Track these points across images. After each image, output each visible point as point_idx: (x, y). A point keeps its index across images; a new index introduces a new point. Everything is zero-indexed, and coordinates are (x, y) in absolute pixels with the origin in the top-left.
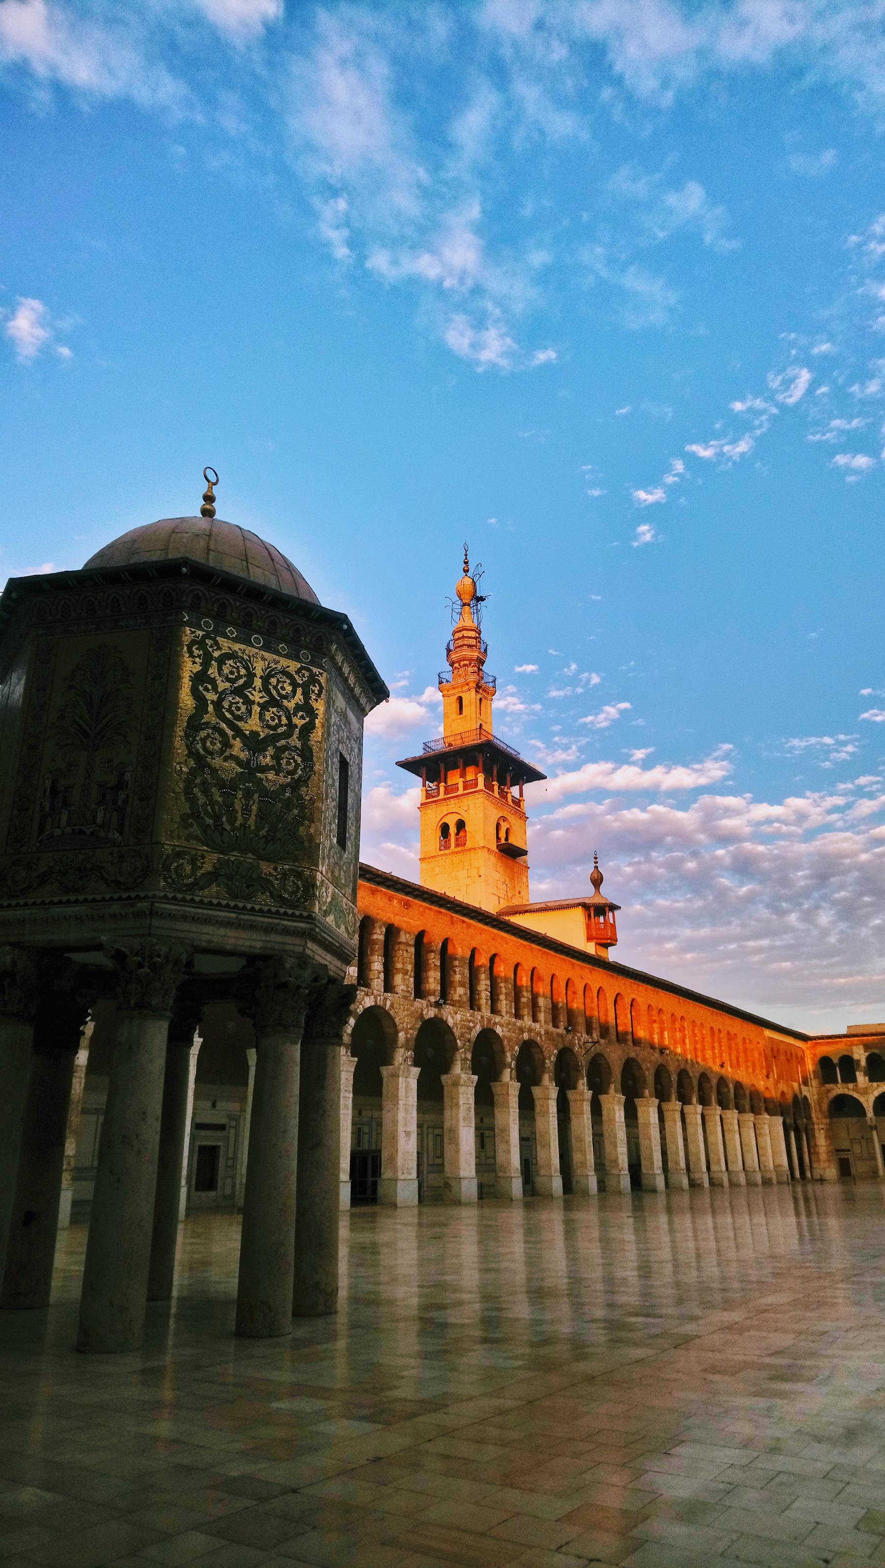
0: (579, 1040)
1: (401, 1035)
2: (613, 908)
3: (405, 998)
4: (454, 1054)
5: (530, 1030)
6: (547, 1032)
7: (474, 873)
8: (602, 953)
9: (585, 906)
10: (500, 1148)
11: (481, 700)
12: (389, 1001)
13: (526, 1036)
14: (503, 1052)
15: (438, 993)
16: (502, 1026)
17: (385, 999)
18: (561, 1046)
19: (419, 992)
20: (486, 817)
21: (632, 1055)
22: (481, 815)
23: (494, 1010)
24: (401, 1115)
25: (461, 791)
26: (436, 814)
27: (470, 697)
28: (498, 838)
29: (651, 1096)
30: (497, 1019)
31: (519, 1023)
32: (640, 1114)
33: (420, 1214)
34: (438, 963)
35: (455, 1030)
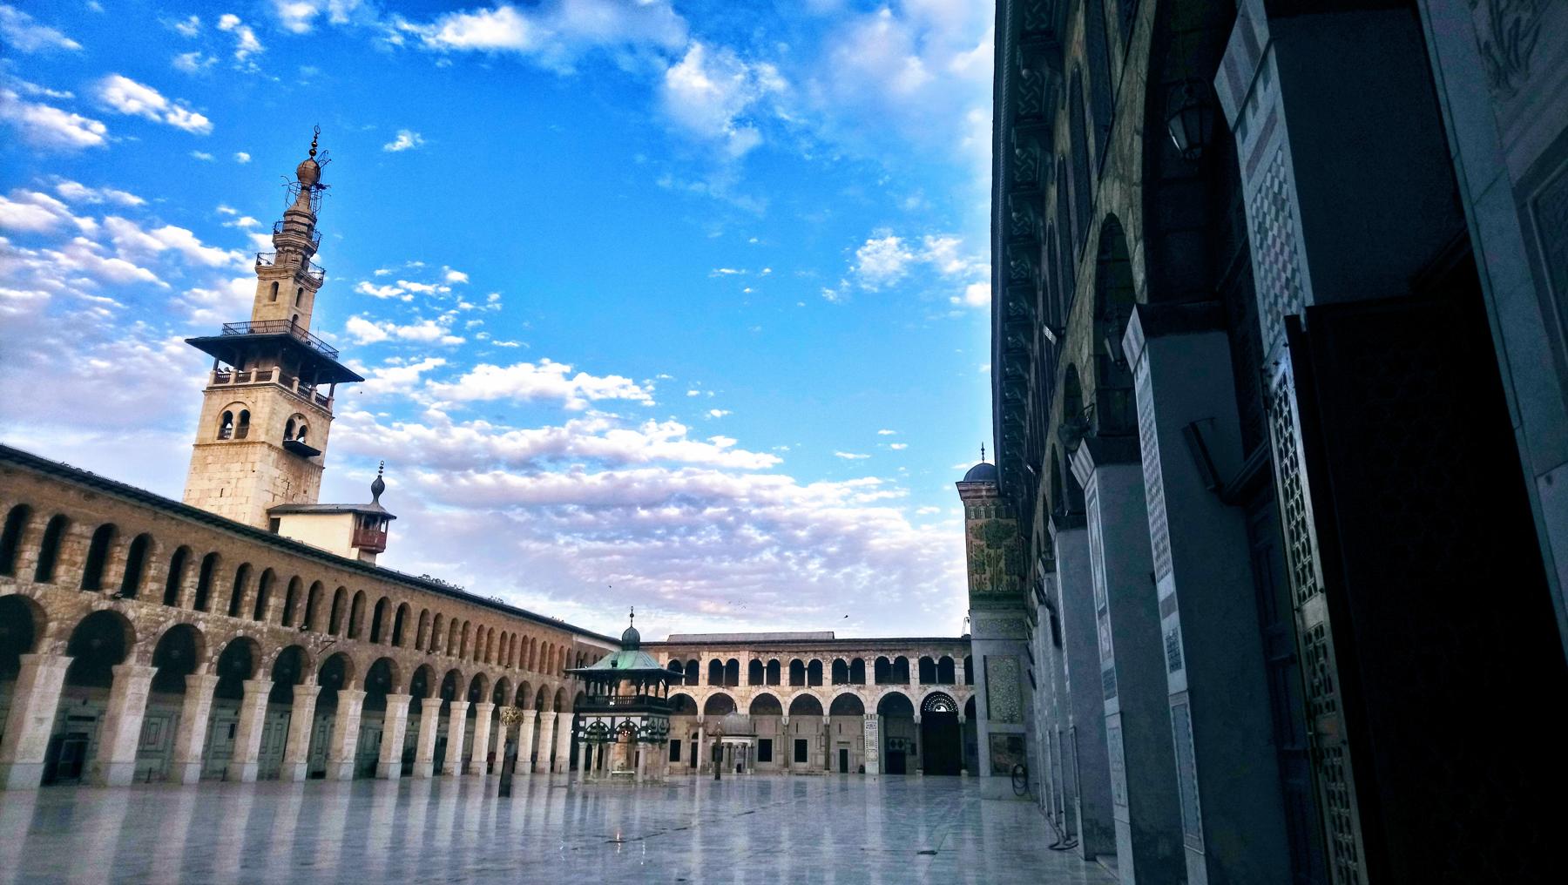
0: (317, 638)
1: (53, 626)
2: (386, 518)
3: (66, 588)
4: (131, 647)
5: (247, 627)
6: (271, 631)
7: (249, 466)
8: (367, 559)
9: (357, 513)
10: (183, 735)
11: (301, 291)
12: (40, 591)
13: (240, 633)
14: (204, 647)
15: (118, 588)
16: (207, 622)
17: (35, 589)
18: (288, 644)
19: (93, 580)
20: (273, 412)
21: (388, 654)
22: (267, 410)
23: (201, 603)
24: (34, 701)
25: (231, 383)
26: (220, 402)
27: (288, 286)
28: (288, 432)
29: (403, 692)
30: (202, 615)
31: (233, 620)
32: (389, 707)
33: (41, 796)
34: (125, 557)
35: (135, 624)
